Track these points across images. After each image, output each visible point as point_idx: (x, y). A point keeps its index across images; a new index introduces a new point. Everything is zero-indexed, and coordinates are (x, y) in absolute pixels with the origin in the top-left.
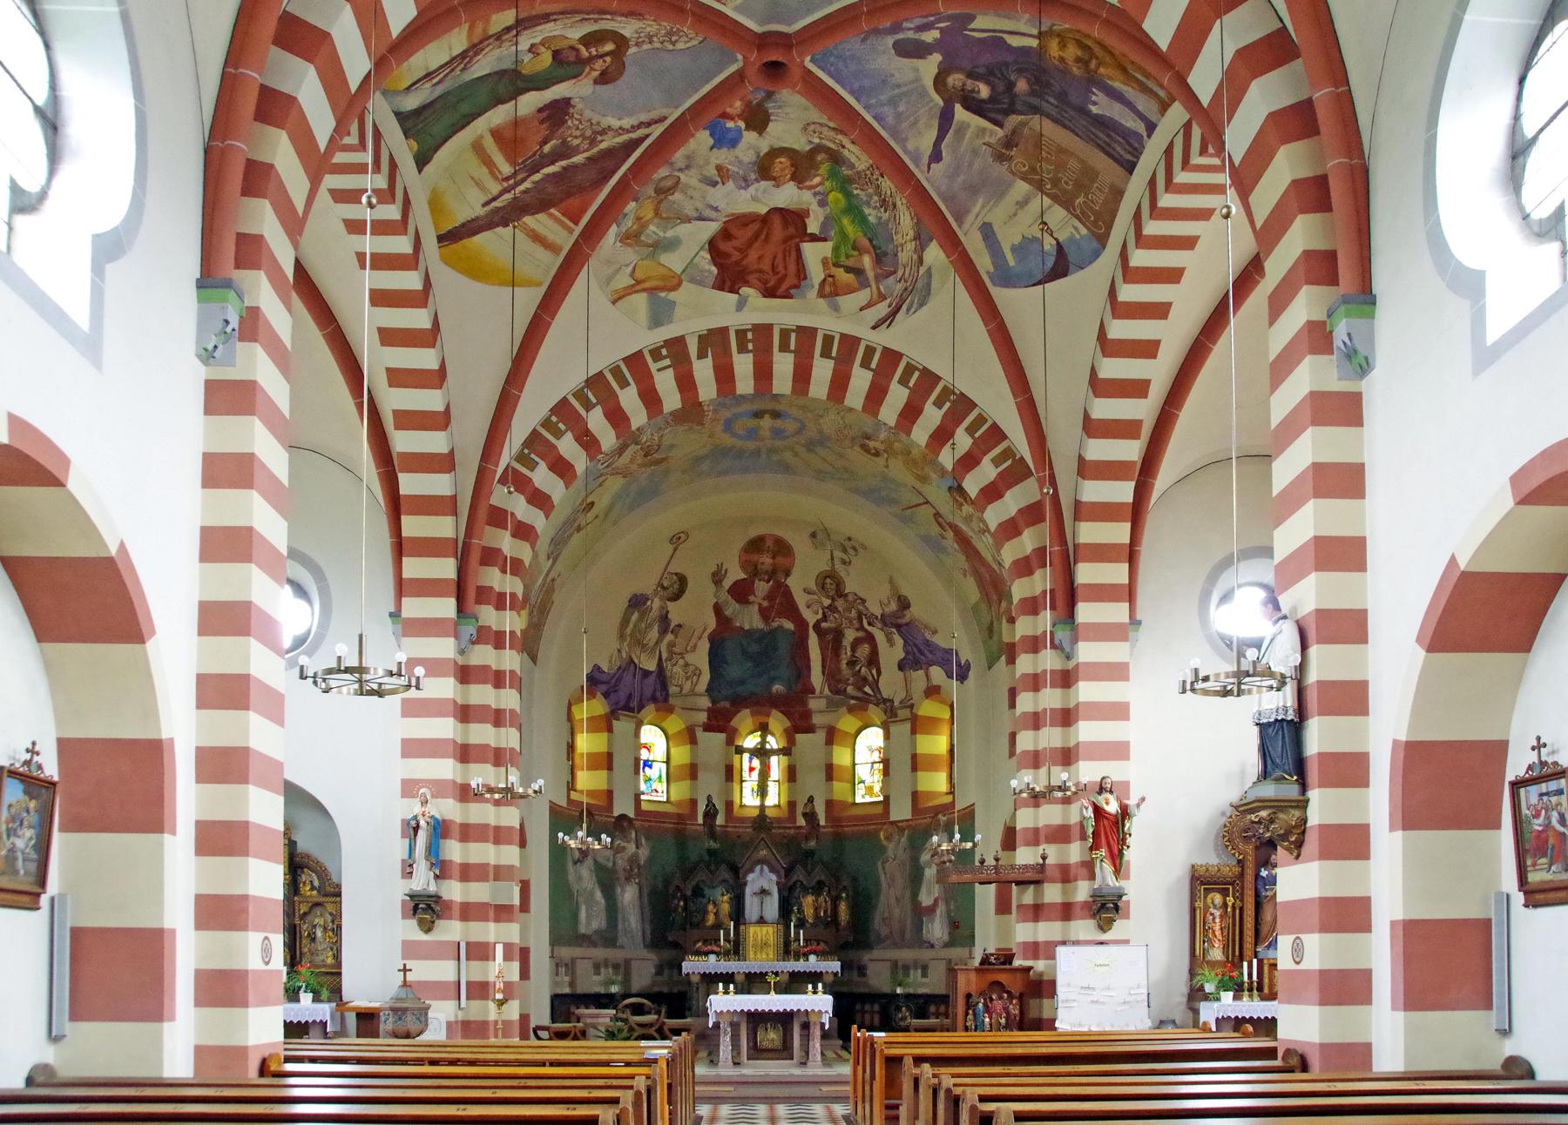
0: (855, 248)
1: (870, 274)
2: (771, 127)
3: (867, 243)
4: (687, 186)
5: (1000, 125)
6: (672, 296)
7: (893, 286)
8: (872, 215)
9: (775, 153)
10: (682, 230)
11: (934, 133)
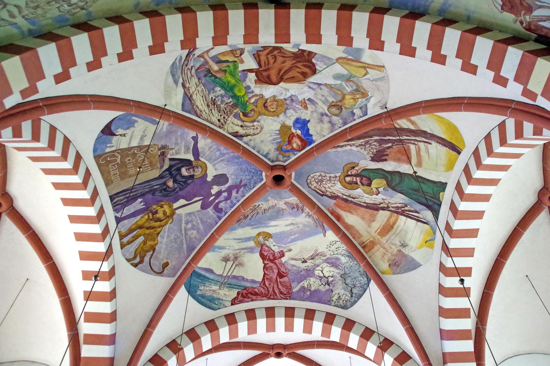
0: (225, 71)
1: (211, 63)
2: (278, 127)
3: (218, 75)
4: (324, 102)
5: (171, 160)
6: (344, 55)
7: (194, 63)
8: (219, 91)
9: (276, 114)
10: (332, 82)
11: (199, 145)
